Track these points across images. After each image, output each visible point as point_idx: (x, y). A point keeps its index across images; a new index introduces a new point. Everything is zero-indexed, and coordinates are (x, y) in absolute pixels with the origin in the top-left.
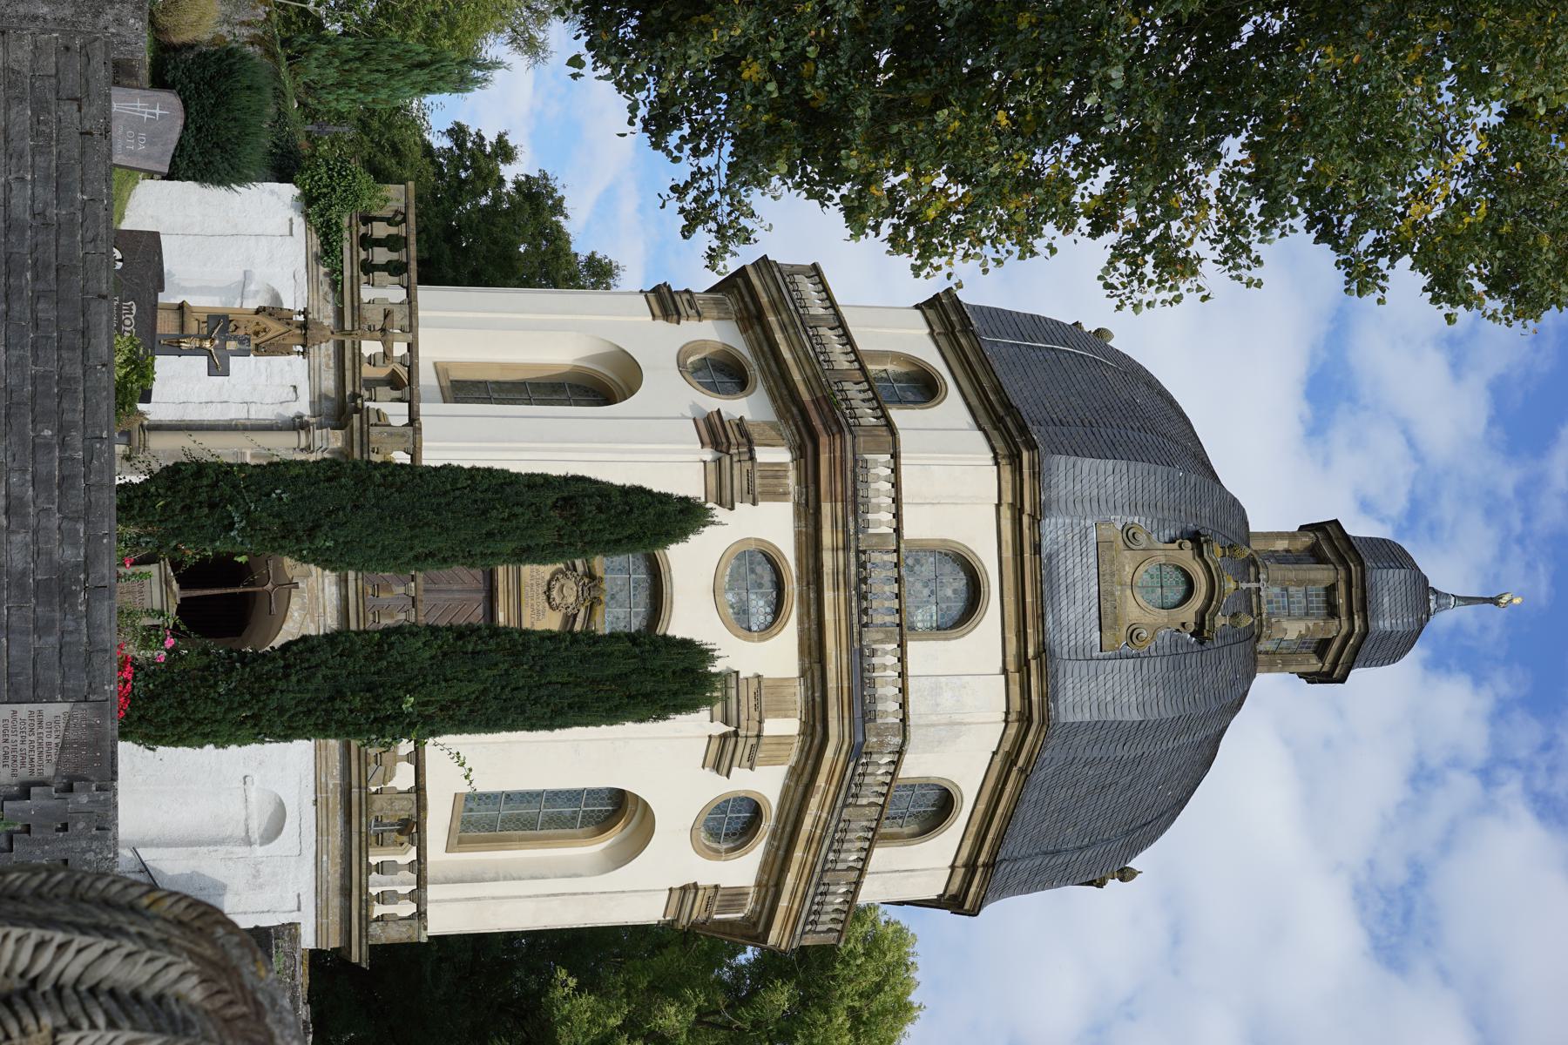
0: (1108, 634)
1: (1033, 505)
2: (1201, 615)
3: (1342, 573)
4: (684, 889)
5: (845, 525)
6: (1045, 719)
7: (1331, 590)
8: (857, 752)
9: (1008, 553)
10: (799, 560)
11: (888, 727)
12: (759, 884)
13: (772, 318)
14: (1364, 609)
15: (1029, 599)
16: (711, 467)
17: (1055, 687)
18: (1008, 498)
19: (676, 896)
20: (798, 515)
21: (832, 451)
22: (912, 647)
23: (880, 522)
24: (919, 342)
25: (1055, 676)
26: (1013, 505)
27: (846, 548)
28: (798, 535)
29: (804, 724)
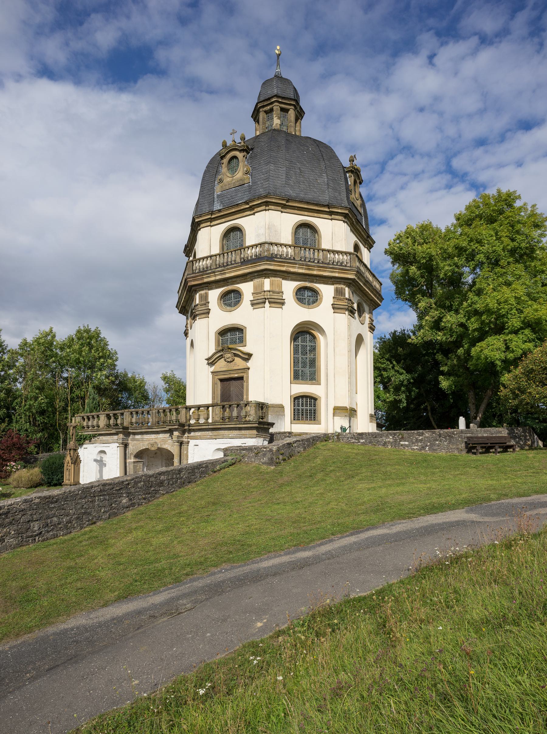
3: (261, 110)
4: (333, 308)
5: (208, 274)
6: (266, 197)
9: (223, 220)
10: (223, 287)
12: (333, 284)
15: (234, 210)
16: (200, 317)
18: (209, 224)
19: (336, 311)
20: (211, 289)
28: (217, 288)
29: (266, 278)
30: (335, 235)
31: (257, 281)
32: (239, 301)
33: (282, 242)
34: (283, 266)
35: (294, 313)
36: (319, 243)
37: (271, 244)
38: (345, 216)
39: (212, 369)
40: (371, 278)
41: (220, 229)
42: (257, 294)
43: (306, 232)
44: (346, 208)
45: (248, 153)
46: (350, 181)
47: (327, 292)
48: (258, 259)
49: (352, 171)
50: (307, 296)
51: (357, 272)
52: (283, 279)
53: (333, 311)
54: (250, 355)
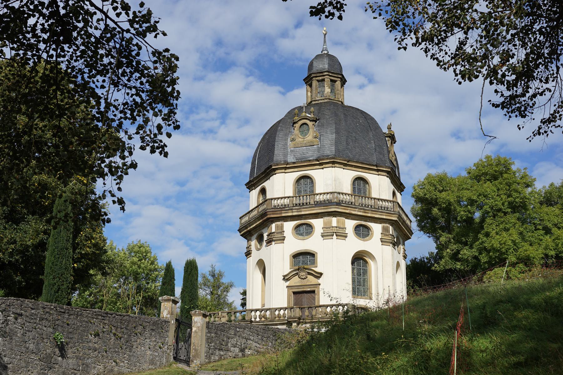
0: (315, 144)
1: (284, 164)
2: (311, 121)
3: (314, 79)
4: (382, 241)
6: (333, 158)
7: (318, 81)
8: (339, 204)
9: (296, 170)
11: (333, 197)
12: (381, 223)
13: (249, 229)
14: (322, 72)
16: (276, 242)
17: (326, 156)
18: (283, 171)
19: (384, 243)
21: (271, 214)
22: (317, 192)
23: (286, 201)
24: (255, 192)
25: (323, 156)
26: (285, 170)
27: (292, 209)
28: (291, 221)
30: (380, 186)
31: (327, 219)
32: (311, 232)
33: (344, 192)
34: (347, 210)
35: (353, 244)
36: (370, 193)
37: (339, 193)
39: (288, 283)
40: (405, 218)
41: (294, 175)
42: (327, 228)
43: (360, 183)
44: (389, 168)
45: (316, 122)
46: (389, 143)
47: (377, 228)
48: (328, 203)
49: (389, 137)
50: (362, 231)
51: (399, 215)
52: (346, 218)
53: (381, 243)
54: (321, 274)
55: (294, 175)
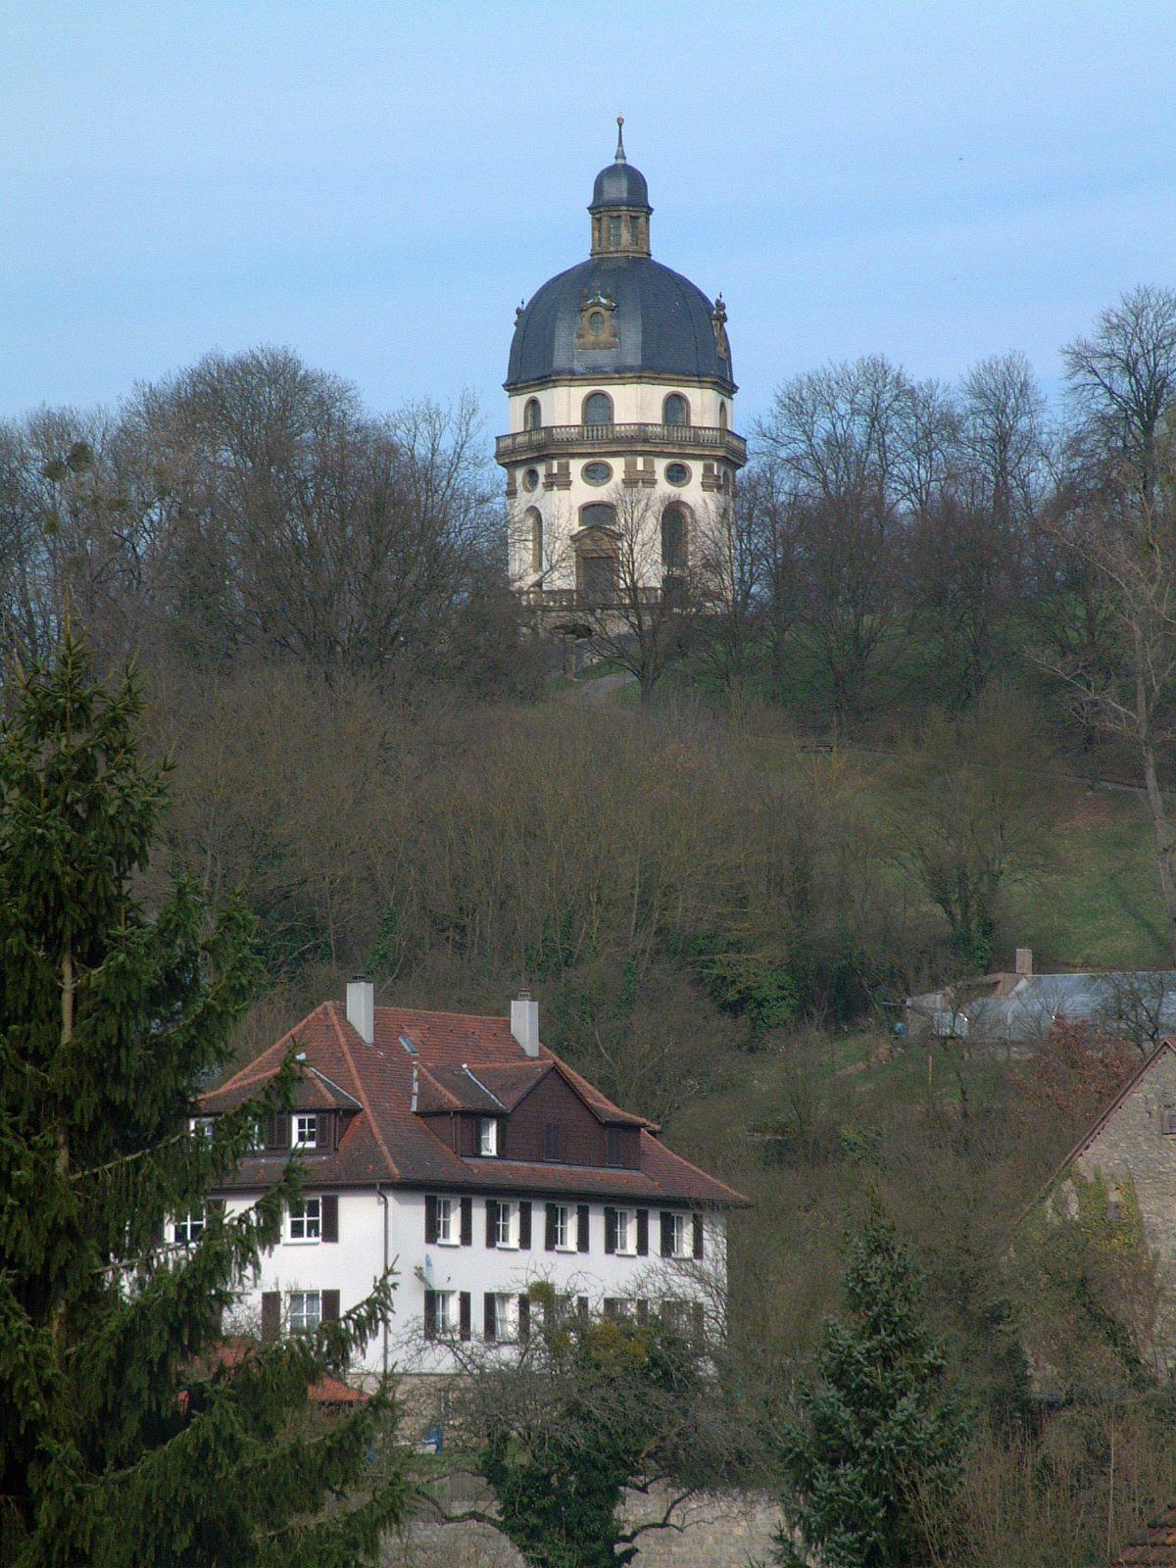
38: (715, 383)
43: (675, 405)
47: (696, 468)
50: (678, 474)
55: (580, 393)
